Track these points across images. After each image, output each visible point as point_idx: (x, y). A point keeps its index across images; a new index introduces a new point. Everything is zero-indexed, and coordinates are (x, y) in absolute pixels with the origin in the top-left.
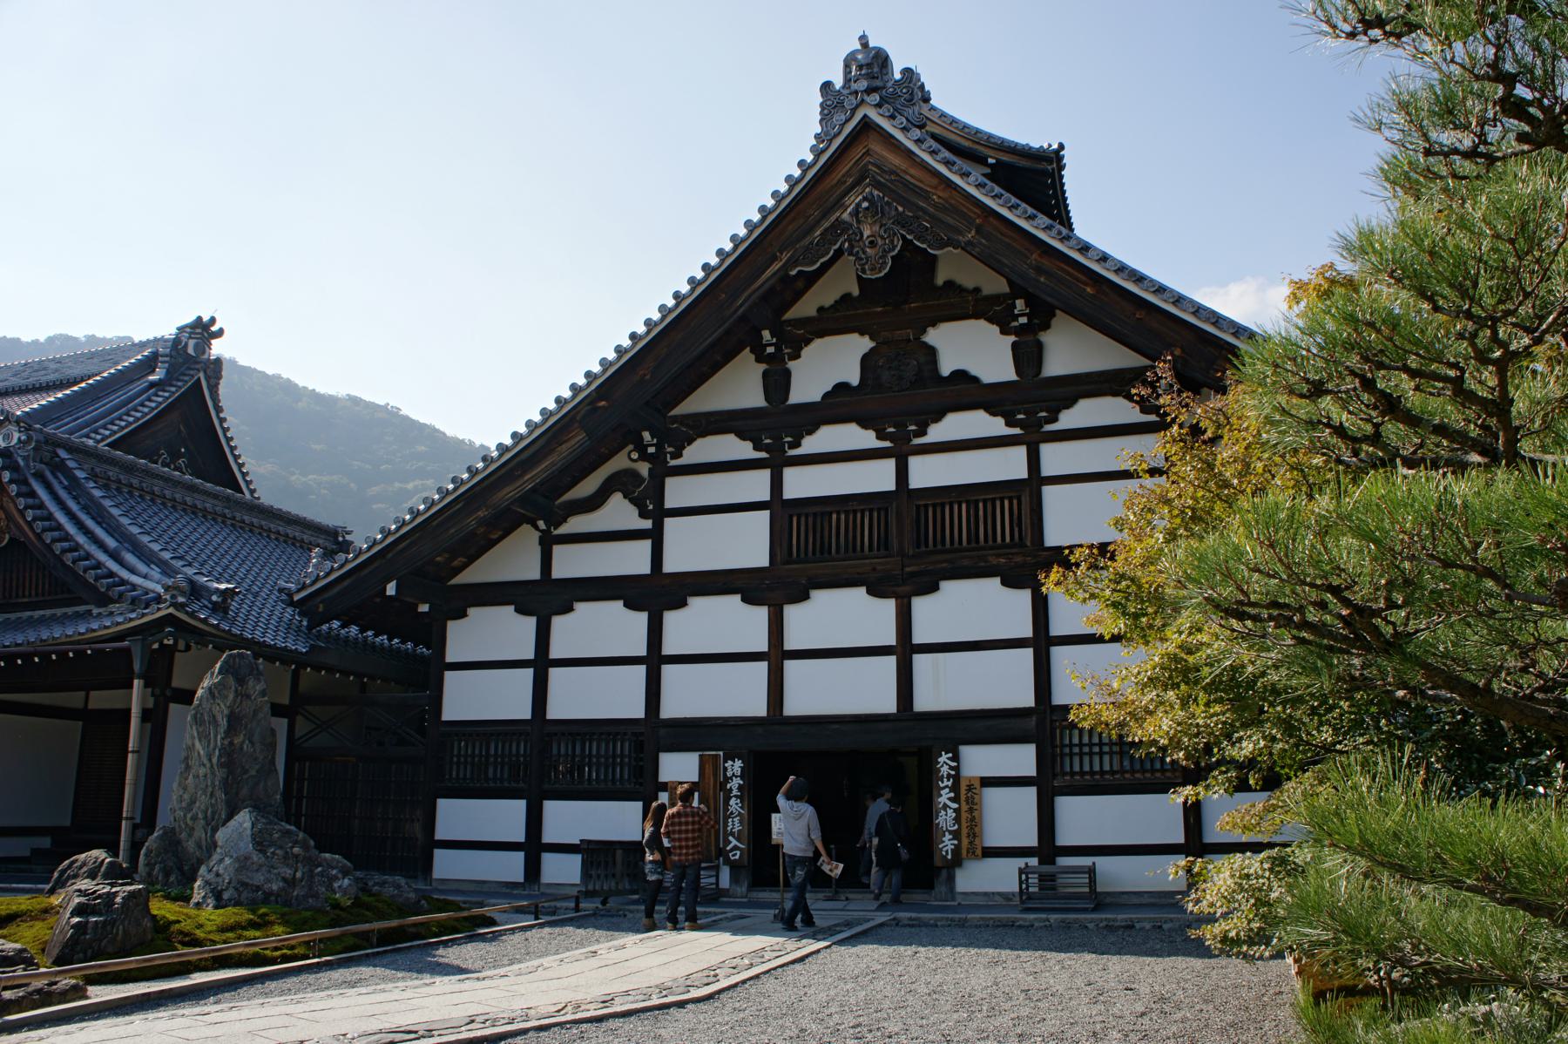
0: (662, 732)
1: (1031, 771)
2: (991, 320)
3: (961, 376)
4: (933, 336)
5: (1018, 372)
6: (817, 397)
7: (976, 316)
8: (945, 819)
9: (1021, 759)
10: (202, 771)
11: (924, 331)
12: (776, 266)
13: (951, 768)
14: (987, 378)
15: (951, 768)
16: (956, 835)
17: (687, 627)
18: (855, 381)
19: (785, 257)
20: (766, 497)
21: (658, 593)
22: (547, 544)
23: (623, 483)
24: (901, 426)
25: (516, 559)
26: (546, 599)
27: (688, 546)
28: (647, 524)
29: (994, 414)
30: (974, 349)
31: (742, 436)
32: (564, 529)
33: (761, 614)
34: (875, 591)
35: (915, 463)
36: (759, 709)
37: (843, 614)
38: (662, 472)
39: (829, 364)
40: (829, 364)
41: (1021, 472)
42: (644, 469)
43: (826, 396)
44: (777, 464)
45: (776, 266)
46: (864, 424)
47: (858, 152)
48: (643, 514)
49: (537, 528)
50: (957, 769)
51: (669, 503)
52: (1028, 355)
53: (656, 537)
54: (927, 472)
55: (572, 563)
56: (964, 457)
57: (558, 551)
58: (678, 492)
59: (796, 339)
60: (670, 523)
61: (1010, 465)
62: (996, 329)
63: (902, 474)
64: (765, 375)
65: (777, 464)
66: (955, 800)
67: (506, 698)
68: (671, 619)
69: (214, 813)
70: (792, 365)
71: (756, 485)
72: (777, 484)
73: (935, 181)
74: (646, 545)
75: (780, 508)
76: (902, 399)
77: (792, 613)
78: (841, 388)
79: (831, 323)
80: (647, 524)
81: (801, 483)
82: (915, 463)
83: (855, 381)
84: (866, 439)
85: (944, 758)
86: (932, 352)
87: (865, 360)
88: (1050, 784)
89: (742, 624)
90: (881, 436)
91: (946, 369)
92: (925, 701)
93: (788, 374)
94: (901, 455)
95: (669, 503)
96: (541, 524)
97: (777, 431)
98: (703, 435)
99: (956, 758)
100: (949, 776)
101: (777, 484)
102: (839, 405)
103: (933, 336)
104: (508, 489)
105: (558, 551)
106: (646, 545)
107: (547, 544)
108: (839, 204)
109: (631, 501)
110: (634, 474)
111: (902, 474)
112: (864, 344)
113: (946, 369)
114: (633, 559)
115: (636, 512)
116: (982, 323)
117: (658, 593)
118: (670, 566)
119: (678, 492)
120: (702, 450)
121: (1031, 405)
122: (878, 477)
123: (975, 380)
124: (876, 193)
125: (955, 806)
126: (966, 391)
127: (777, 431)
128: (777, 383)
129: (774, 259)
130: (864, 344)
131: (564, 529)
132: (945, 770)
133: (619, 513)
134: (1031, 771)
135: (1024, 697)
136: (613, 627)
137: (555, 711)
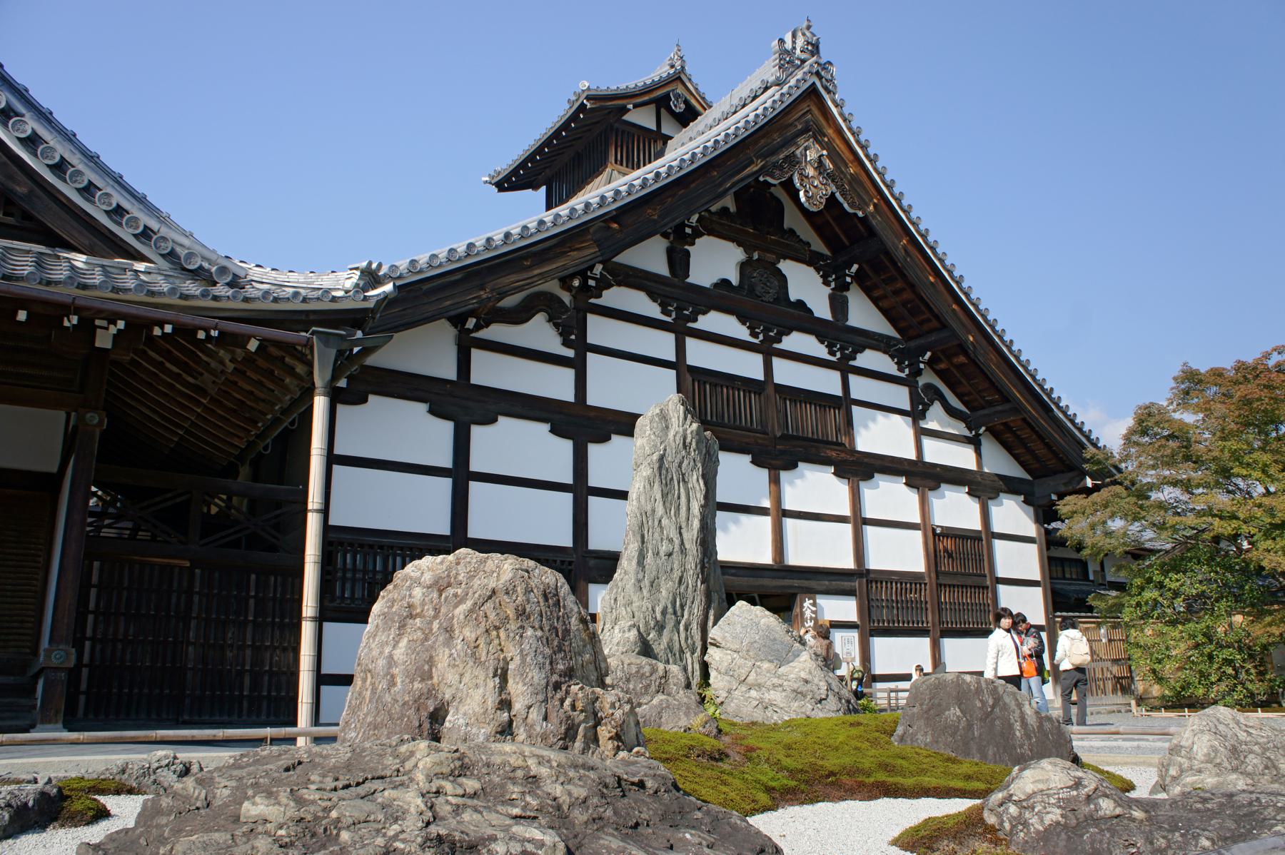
0: (592, 562)
1: (853, 616)
3: (801, 304)
7: (809, 264)
9: (844, 608)
10: (664, 548)
14: (817, 314)
18: (734, 279)
24: (766, 330)
25: (430, 352)
26: (465, 405)
28: (570, 353)
30: (806, 286)
31: (653, 296)
32: (484, 334)
42: (566, 298)
43: (716, 285)
44: (682, 331)
46: (742, 319)
47: (804, 107)
48: (566, 343)
49: (458, 321)
51: (592, 339)
52: (839, 305)
54: (787, 374)
55: (490, 371)
57: (477, 356)
58: (599, 330)
60: (591, 358)
61: (828, 382)
65: (682, 331)
68: (595, 451)
71: (663, 345)
72: (681, 349)
73: (851, 158)
78: (725, 283)
80: (570, 353)
81: (701, 355)
82: (777, 362)
83: (734, 279)
84: (742, 333)
85: (808, 603)
86: (783, 279)
87: (743, 266)
93: (688, 254)
94: (768, 351)
99: (814, 604)
100: (811, 618)
101: (681, 349)
102: (721, 297)
103: (786, 266)
104: (513, 278)
105: (477, 356)
106: (569, 374)
108: (791, 141)
109: (556, 326)
113: (793, 297)
114: (555, 384)
115: (558, 340)
116: (811, 270)
118: (595, 398)
119: (599, 330)
120: (617, 297)
121: (843, 343)
122: (749, 366)
123: (810, 311)
126: (801, 318)
127: (681, 304)
128: (679, 261)
129: (751, 163)
131: (484, 334)
132: (808, 614)
135: (848, 563)
136: (547, 453)
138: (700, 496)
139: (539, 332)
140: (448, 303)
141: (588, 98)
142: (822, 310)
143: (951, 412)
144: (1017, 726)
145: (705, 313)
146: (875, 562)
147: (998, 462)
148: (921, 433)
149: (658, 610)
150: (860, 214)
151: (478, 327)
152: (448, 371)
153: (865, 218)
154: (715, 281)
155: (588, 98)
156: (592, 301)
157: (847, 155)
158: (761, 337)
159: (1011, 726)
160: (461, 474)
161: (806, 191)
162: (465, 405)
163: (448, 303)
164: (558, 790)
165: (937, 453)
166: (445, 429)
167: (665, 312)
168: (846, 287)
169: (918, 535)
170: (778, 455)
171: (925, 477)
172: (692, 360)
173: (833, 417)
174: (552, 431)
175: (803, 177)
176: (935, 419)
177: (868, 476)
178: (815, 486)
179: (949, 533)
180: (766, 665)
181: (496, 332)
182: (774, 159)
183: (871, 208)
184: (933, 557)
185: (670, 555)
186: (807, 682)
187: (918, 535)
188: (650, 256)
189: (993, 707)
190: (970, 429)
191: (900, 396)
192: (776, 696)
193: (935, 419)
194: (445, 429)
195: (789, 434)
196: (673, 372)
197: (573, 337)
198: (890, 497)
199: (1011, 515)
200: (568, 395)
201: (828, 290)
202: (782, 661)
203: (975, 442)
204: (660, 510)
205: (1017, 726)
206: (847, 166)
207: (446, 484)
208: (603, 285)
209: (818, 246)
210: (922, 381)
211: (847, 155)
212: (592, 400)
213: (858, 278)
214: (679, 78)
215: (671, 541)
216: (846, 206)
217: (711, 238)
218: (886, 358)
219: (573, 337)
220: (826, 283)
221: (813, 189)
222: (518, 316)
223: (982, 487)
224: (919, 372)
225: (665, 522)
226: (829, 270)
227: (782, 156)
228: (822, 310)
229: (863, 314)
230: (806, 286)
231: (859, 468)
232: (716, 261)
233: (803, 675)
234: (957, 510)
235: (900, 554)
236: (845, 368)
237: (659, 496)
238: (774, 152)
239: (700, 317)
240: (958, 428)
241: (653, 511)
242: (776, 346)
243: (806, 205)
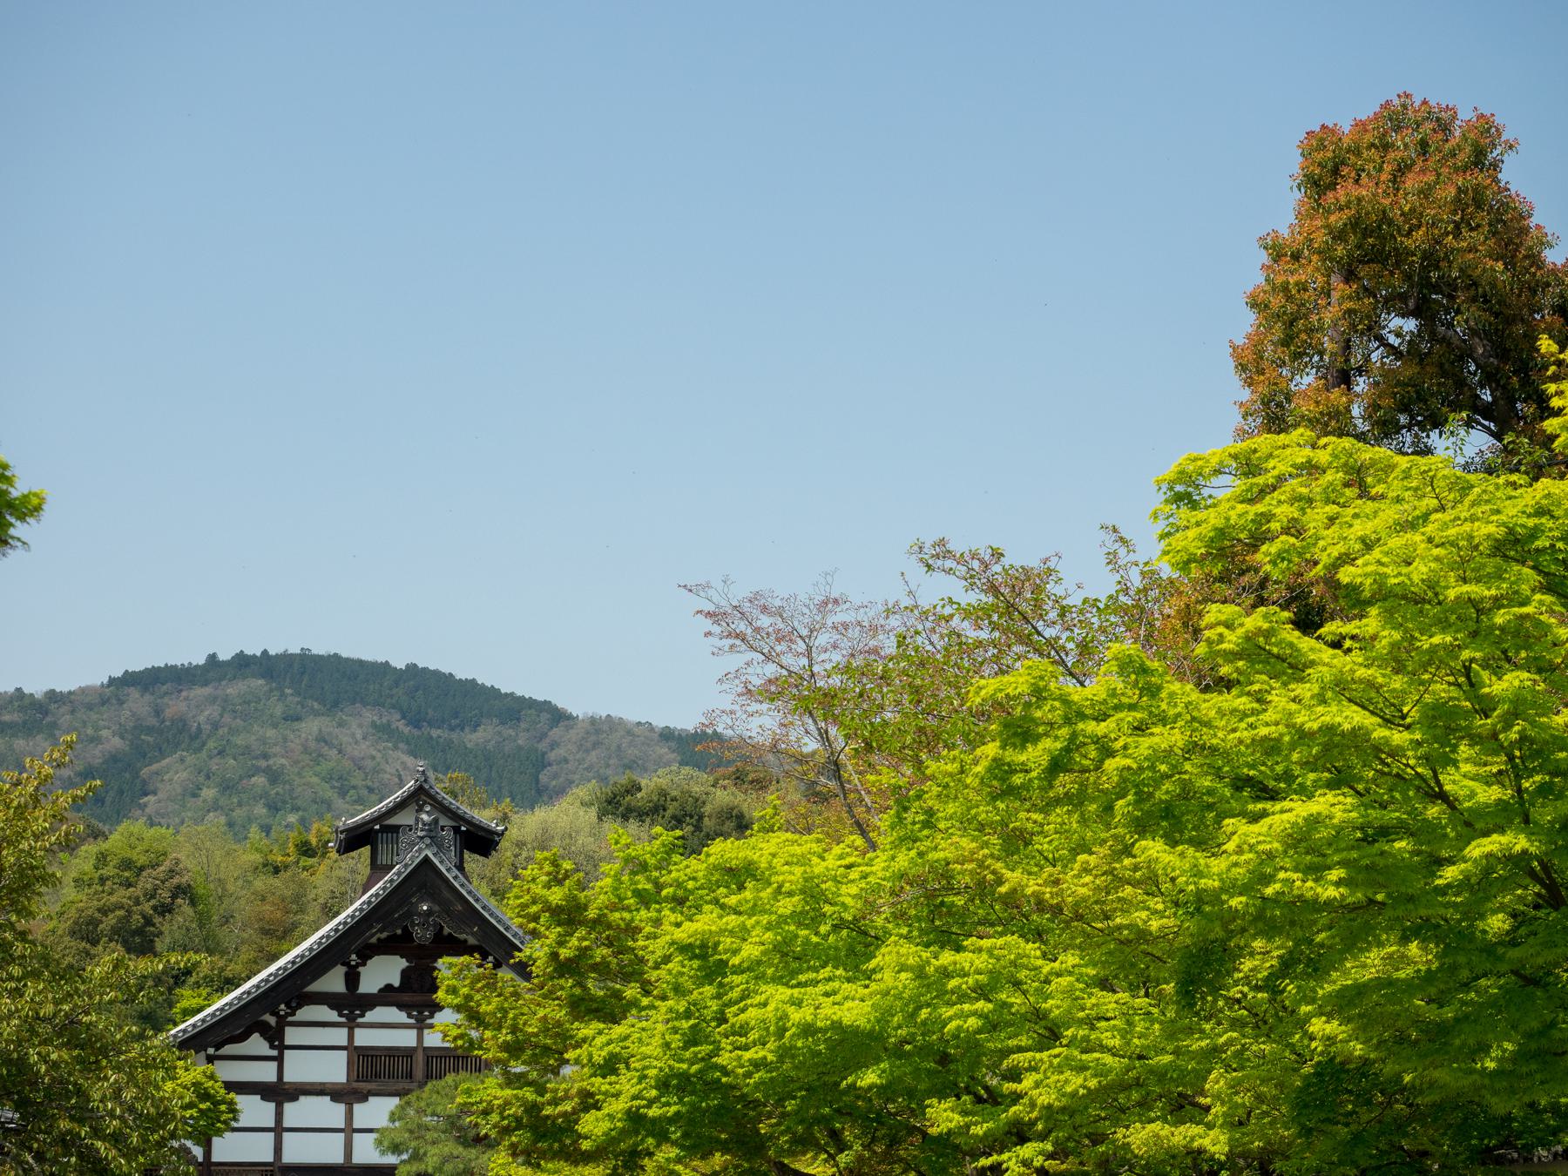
6: (375, 991)
17: (295, 1113)
18: (397, 984)
24: (420, 1013)
27: (299, 1068)
28: (275, 1053)
32: (222, 1051)
33: (340, 1108)
38: (283, 1023)
40: (383, 972)
44: (351, 1025)
46: (401, 1007)
48: (272, 1047)
53: (280, 1060)
59: (366, 954)
63: (420, 1038)
64: (347, 974)
65: (351, 1025)
68: (288, 1107)
71: (339, 1036)
72: (351, 1037)
74: (274, 1065)
75: (350, 1048)
77: (358, 1108)
78: (388, 988)
79: (386, 947)
80: (275, 1053)
81: (364, 1038)
83: (397, 984)
87: (404, 973)
89: (333, 1113)
90: (409, 1016)
93: (358, 974)
97: (352, 1005)
101: (351, 1037)
102: (387, 996)
106: (274, 1065)
110: (266, 1024)
111: (420, 1038)
112: (403, 963)
114: (265, 1073)
115: (267, 1045)
117: (279, 1093)
118: (288, 1077)
119: (292, 1036)
122: (407, 1039)
127: (352, 1005)
128: (352, 979)
129: (372, 927)
130: (403, 963)
131: (222, 1051)
136: (255, 1110)
137: (216, 1158)
139: (256, 1044)
172: (358, 1043)
181: (229, 1049)
188: (333, 981)
200: (273, 1078)
212: (288, 1077)
222: (243, 1037)
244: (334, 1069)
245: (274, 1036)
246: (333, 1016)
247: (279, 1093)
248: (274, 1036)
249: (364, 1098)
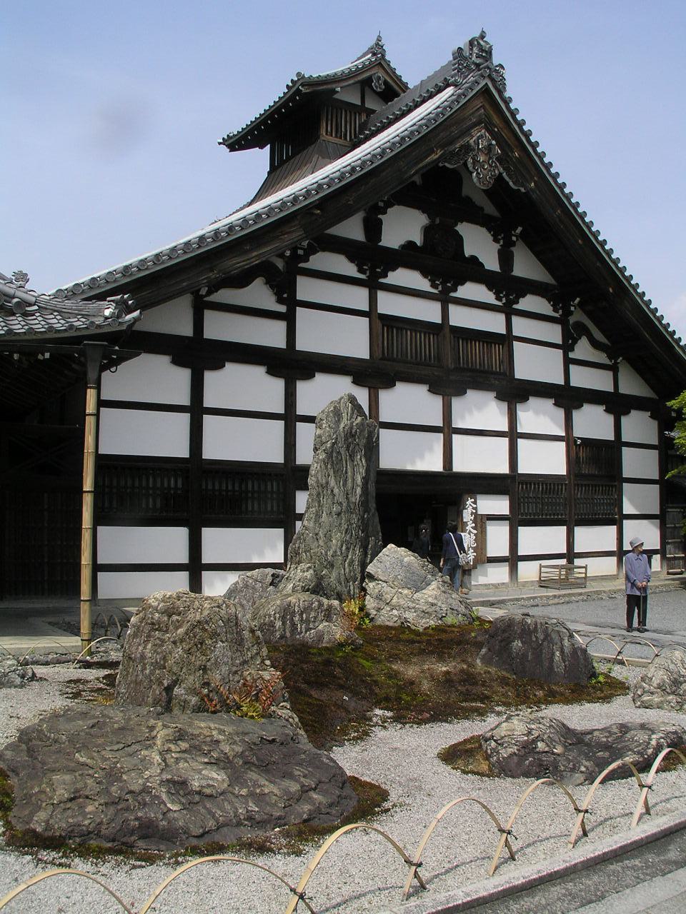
1: (506, 511)
2: (489, 230)
3: (474, 259)
4: (464, 229)
5: (501, 269)
7: (482, 225)
8: (468, 539)
9: (500, 505)
10: (335, 509)
11: (456, 225)
12: (434, 157)
13: (473, 508)
15: (473, 508)
16: (475, 550)
18: (419, 241)
19: (440, 153)
20: (365, 308)
21: (292, 365)
22: (200, 308)
23: (264, 270)
24: (443, 283)
26: (200, 355)
27: (318, 333)
28: (282, 309)
29: (490, 289)
30: (479, 244)
31: (352, 260)
34: (433, 390)
35: (452, 309)
36: (183, 451)
37: (408, 401)
39: (404, 227)
41: (502, 330)
43: (403, 247)
44: (374, 285)
45: (434, 157)
46: (425, 274)
48: (280, 301)
50: (476, 509)
51: (300, 296)
52: (506, 258)
53: (289, 319)
54: (461, 317)
55: (220, 328)
56: (474, 313)
57: (209, 315)
61: (493, 323)
62: (489, 237)
65: (374, 285)
66: (474, 528)
67: (165, 438)
68: (302, 387)
69: (348, 549)
70: (380, 216)
71: (357, 297)
72: (373, 301)
74: (281, 326)
76: (444, 265)
78: (410, 245)
79: (409, 197)
80: (282, 309)
81: (390, 305)
82: (452, 309)
83: (419, 241)
84: (423, 284)
85: (470, 501)
86: (459, 240)
87: (427, 231)
88: (517, 520)
91: (468, 252)
92: (458, 467)
93: (380, 222)
94: (445, 300)
95: (300, 296)
96: (203, 291)
98: (324, 250)
99: (475, 503)
101: (373, 301)
102: (407, 256)
103: (464, 229)
105: (209, 315)
106: (281, 326)
107: (200, 308)
108: (467, 132)
109: (272, 287)
113: (468, 252)
114: (271, 335)
115: (273, 298)
116: (484, 230)
118: (302, 344)
119: (307, 289)
121: (508, 289)
122: (429, 312)
123: (482, 265)
124: (487, 135)
125: (475, 532)
126: (474, 271)
127: (374, 263)
128: (373, 228)
129: (433, 152)
133: (259, 294)
134: (506, 511)
135: (504, 469)
137: (211, 451)
138: (363, 471)
140: (185, 284)
141: (302, 85)
142: (491, 263)
143: (595, 344)
144: (558, 653)
145: (394, 270)
146: (523, 468)
147: (631, 385)
148: (568, 362)
149: (330, 553)
150: (523, 190)
151: (209, 293)
152: (187, 330)
153: (526, 194)
154: (403, 243)
155: (302, 85)
156: (301, 265)
157: (511, 141)
158: (440, 288)
159: (553, 654)
160: (197, 410)
161: (478, 173)
162: (200, 355)
163: (185, 284)
164: (227, 748)
165: (582, 378)
166: (184, 375)
167: (361, 271)
168: (513, 244)
169: (562, 446)
170: (449, 383)
171: (568, 398)
173: (497, 351)
174: (269, 372)
175: (475, 162)
176: (583, 350)
177: (524, 399)
178: (481, 410)
179: (587, 442)
180: (406, 591)
181: (226, 296)
182: (451, 148)
183: (533, 184)
184: (572, 461)
185: (339, 514)
186: (433, 605)
187: (563, 444)
189: (543, 641)
190: (610, 358)
191: (554, 333)
192: (410, 616)
193: (583, 350)
194: (184, 375)
195: (462, 365)
196: (367, 320)
197: (285, 295)
198: (539, 417)
199: (638, 426)
201: (497, 246)
202: (418, 589)
203: (614, 369)
204: (332, 483)
205: (558, 653)
206: (513, 152)
207: (185, 418)
208: (311, 251)
209: (490, 209)
210: (572, 320)
211: (511, 141)
213: (522, 236)
214: (380, 64)
215: (340, 504)
216: (511, 183)
217: (402, 208)
218: (544, 301)
219: (285, 295)
220: (496, 240)
221: (481, 173)
222: (242, 280)
223: (617, 405)
224: (571, 313)
225: (336, 491)
226: (499, 230)
227: (458, 146)
228: (491, 263)
229: (525, 266)
230: (479, 244)
231: (515, 393)
232: (404, 227)
233: (430, 600)
234: (594, 423)
235: (546, 460)
236: (509, 311)
237: (331, 473)
238: (452, 142)
239: (390, 274)
240: (601, 358)
241: (327, 483)
242: (453, 294)
243: (478, 184)
244: (353, 340)
245: (284, 288)
246: (350, 270)
247: (292, 365)
248: (284, 288)
249: (390, 384)
